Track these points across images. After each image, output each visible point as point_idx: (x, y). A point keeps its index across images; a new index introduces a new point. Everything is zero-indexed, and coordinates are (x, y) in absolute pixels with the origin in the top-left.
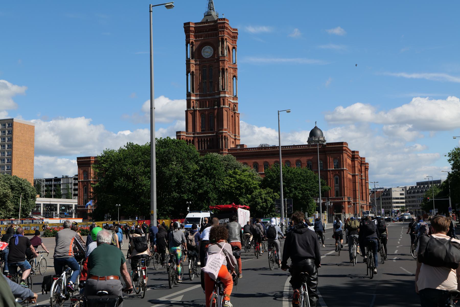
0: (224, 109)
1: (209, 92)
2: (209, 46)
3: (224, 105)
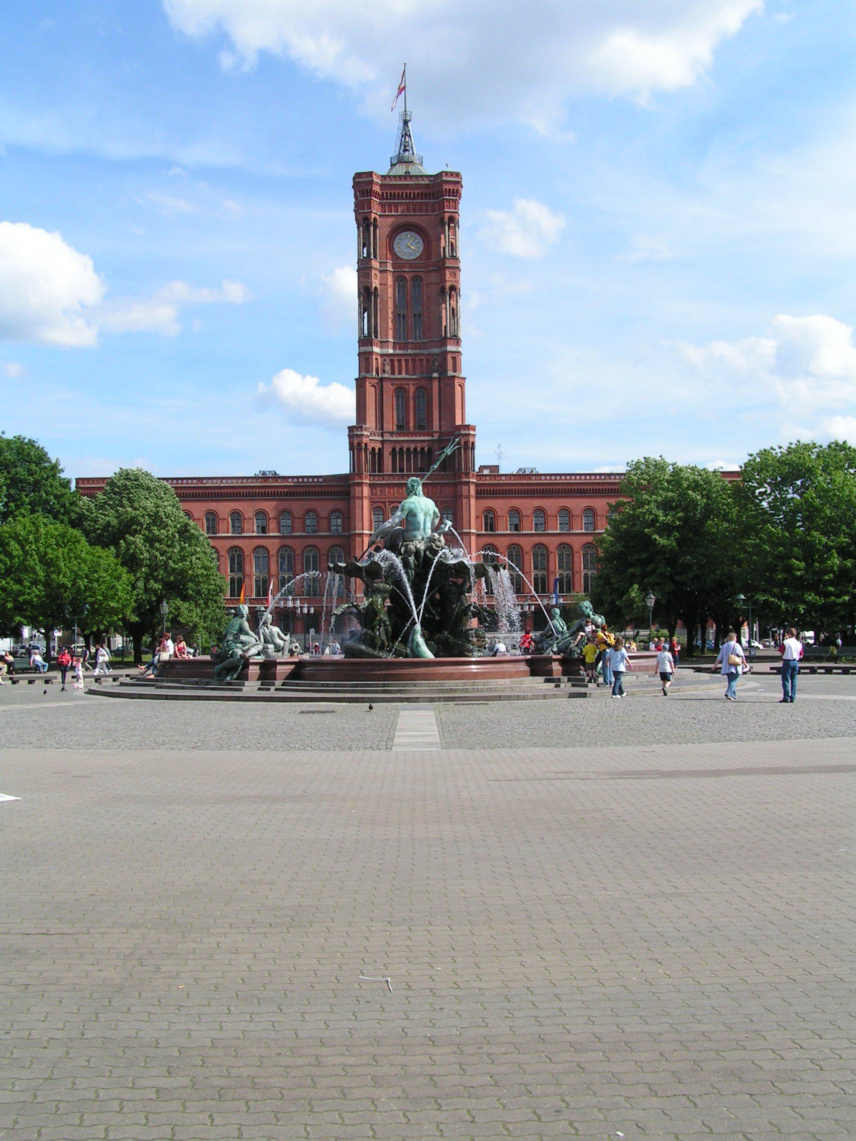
0: (456, 381)
1: (412, 339)
2: (412, 233)
3: (455, 371)
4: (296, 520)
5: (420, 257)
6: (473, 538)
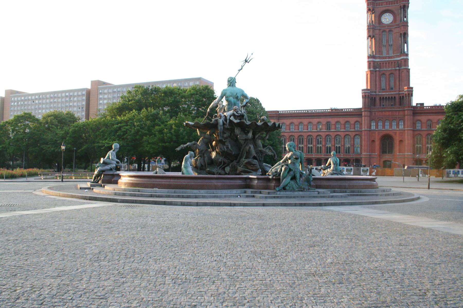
2: (388, 13)
4: (342, 125)
5: (392, 23)
6: (412, 131)
